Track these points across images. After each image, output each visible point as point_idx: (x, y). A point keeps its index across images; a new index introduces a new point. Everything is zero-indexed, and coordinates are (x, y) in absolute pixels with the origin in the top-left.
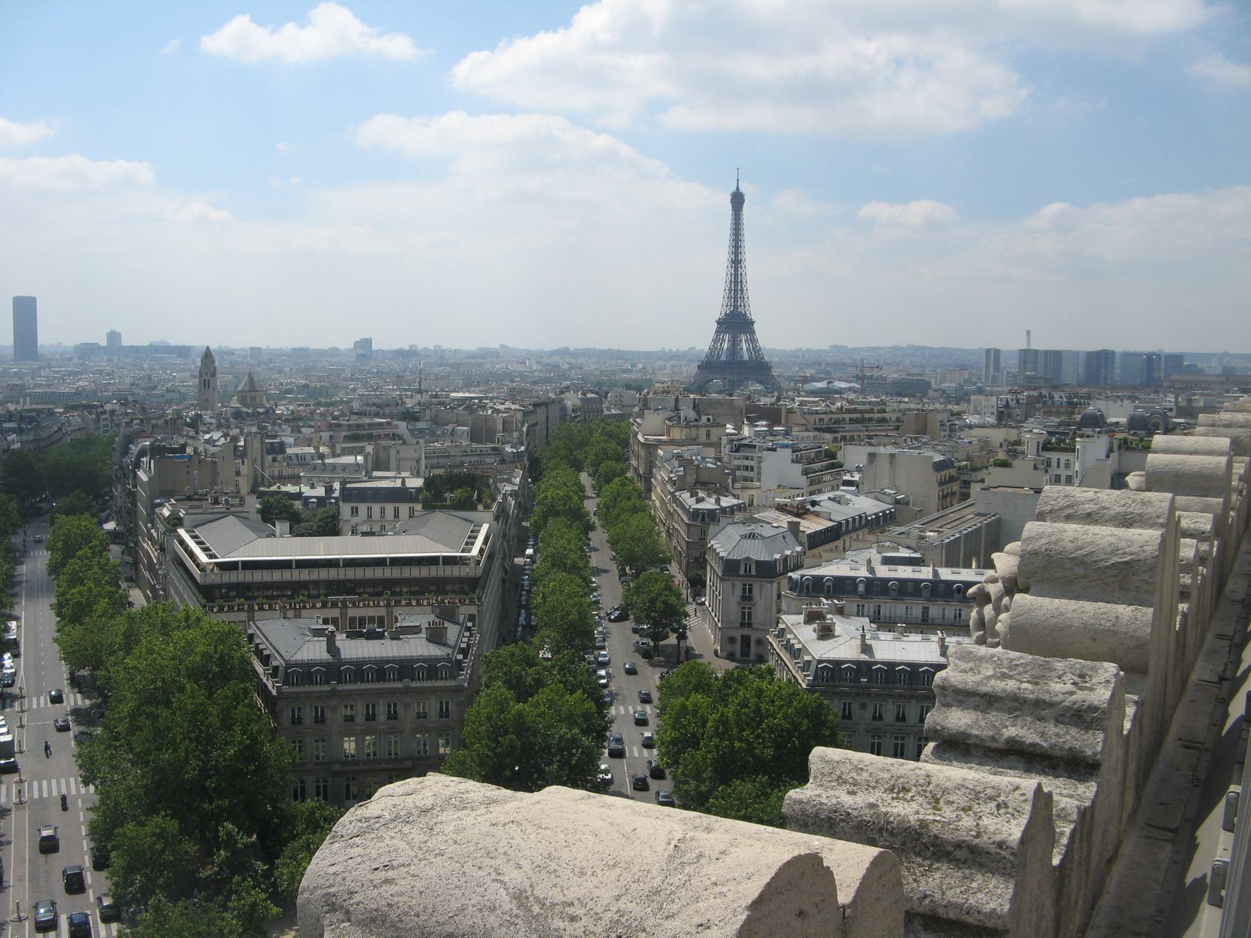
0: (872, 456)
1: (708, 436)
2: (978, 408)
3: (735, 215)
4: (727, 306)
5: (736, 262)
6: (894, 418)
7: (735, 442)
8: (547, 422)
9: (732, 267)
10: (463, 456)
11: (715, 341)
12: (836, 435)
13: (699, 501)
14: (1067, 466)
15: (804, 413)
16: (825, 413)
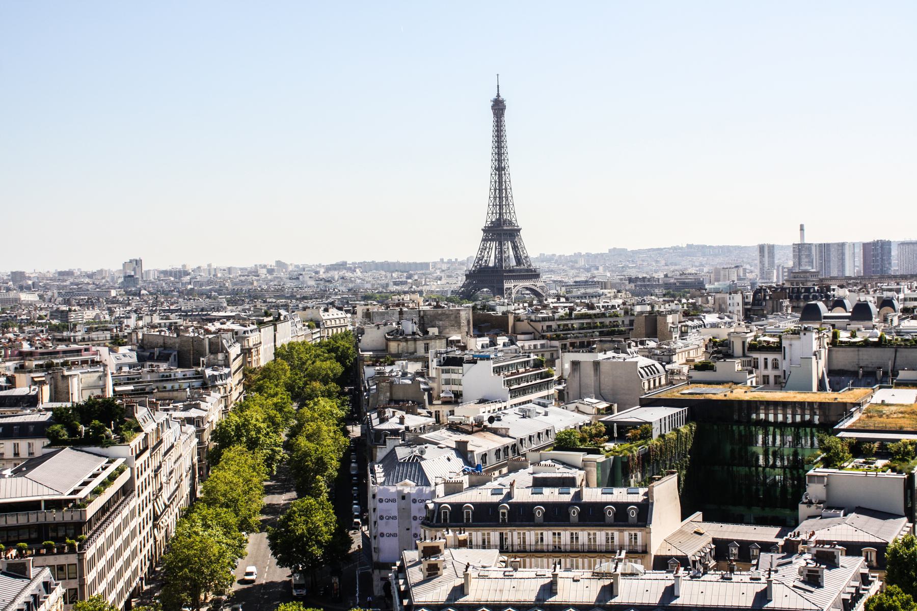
0: (575, 364)
1: (427, 349)
2: (723, 306)
3: (497, 121)
4: (493, 213)
5: (500, 169)
6: (627, 322)
7: (443, 356)
8: (275, 341)
9: (496, 174)
10: (162, 381)
11: (483, 250)
12: (564, 342)
13: (383, 420)
14: (776, 366)
15: (532, 321)
16: (553, 319)
